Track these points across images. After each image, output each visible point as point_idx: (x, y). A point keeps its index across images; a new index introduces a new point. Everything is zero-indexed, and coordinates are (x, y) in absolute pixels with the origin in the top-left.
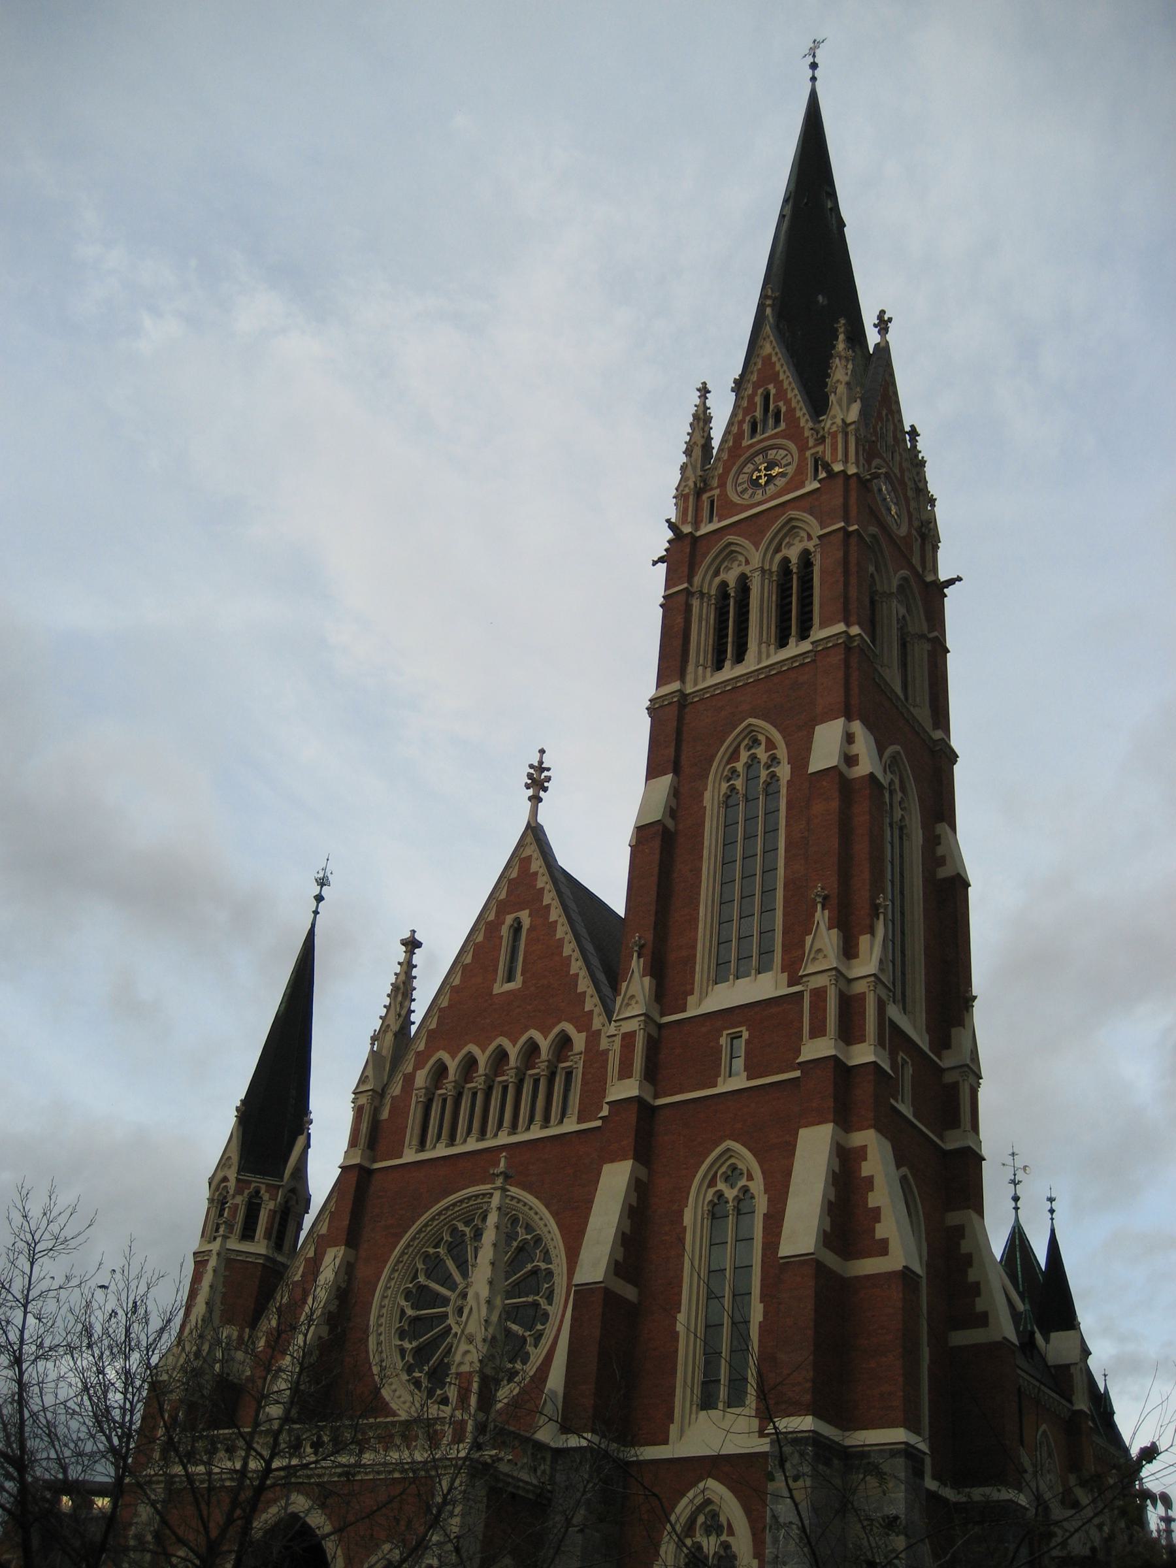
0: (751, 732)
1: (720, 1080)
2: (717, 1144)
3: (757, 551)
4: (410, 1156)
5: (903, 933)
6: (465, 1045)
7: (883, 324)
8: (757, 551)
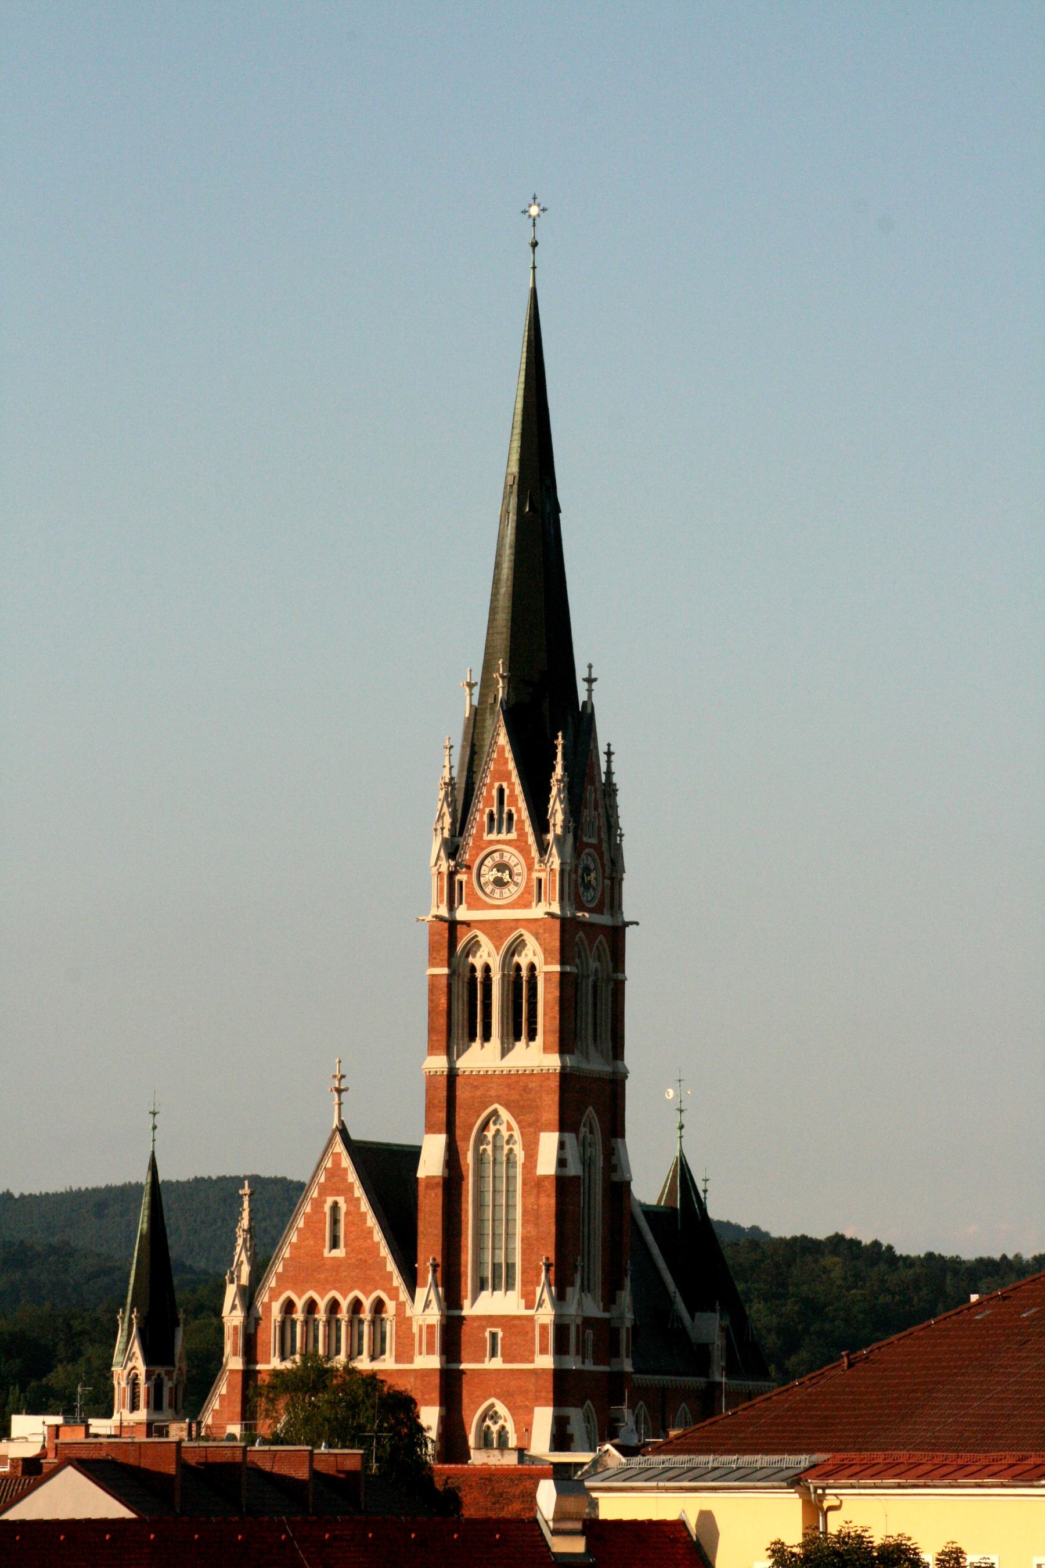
0: (495, 1113)
1: (487, 1359)
2: (486, 1399)
3: (498, 954)
4: (275, 1363)
5: (589, 1279)
6: (308, 1290)
7: (590, 681)
8: (498, 954)
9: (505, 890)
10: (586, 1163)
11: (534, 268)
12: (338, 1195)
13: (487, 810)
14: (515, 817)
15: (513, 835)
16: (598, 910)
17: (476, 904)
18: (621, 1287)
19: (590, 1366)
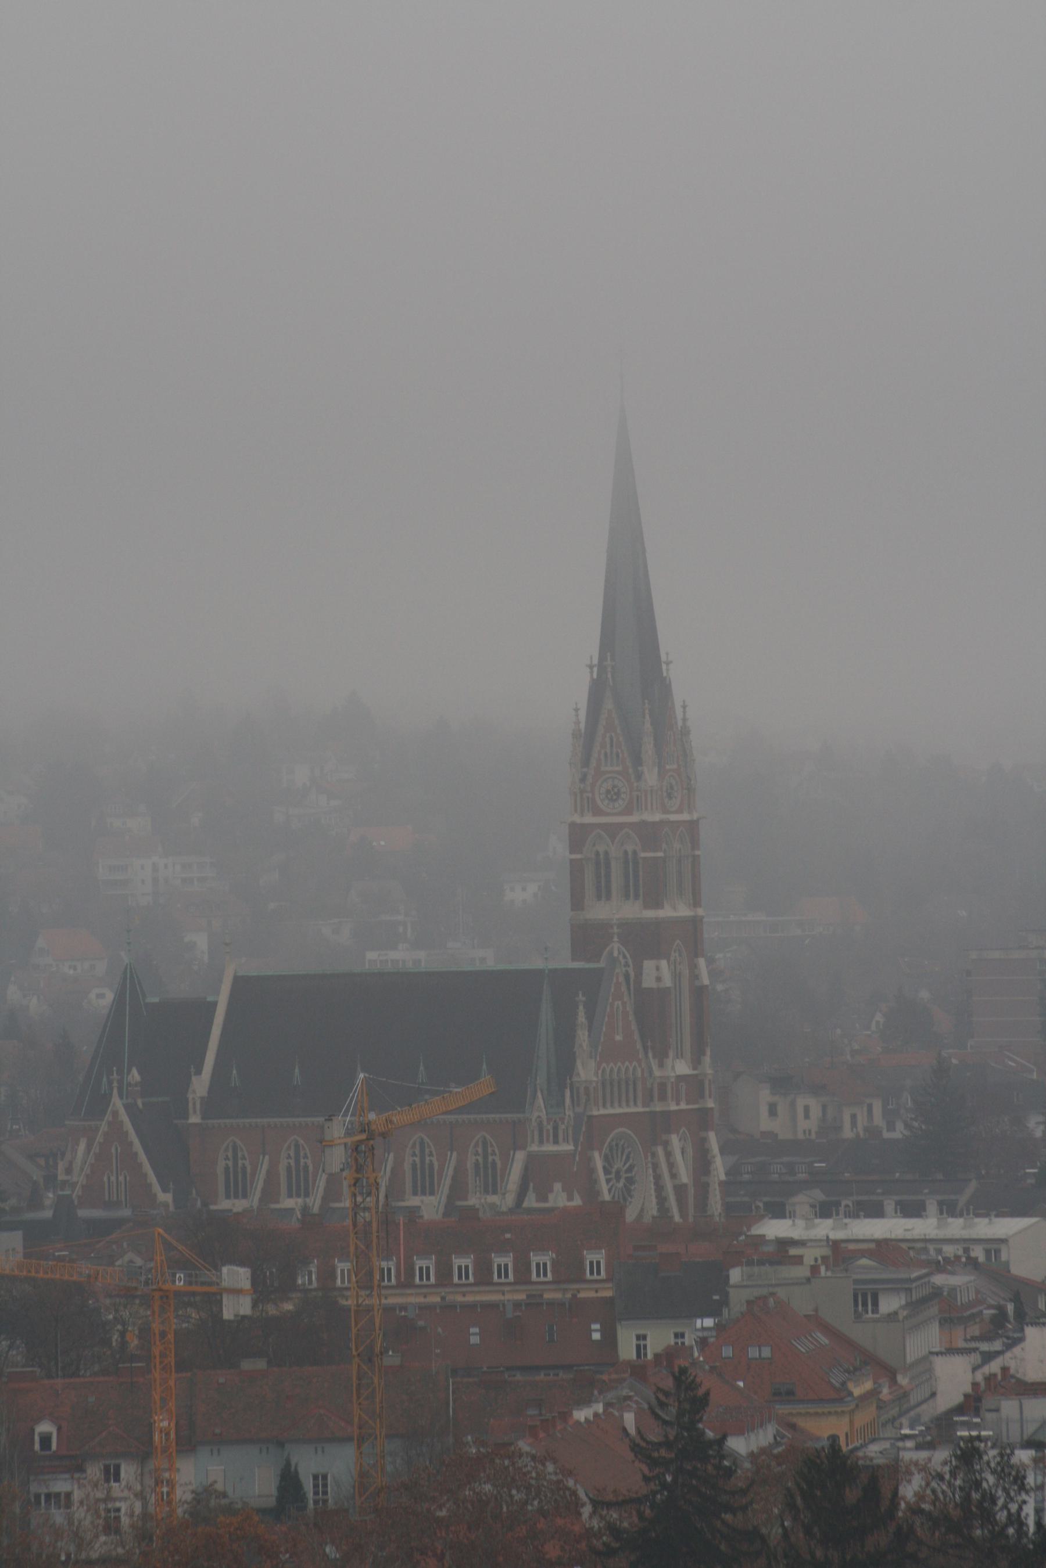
3: (613, 844)
10: (676, 976)
13: (603, 752)
14: (621, 755)
15: (619, 768)
16: (680, 811)
17: (597, 812)
18: (704, 1054)
19: (683, 1106)
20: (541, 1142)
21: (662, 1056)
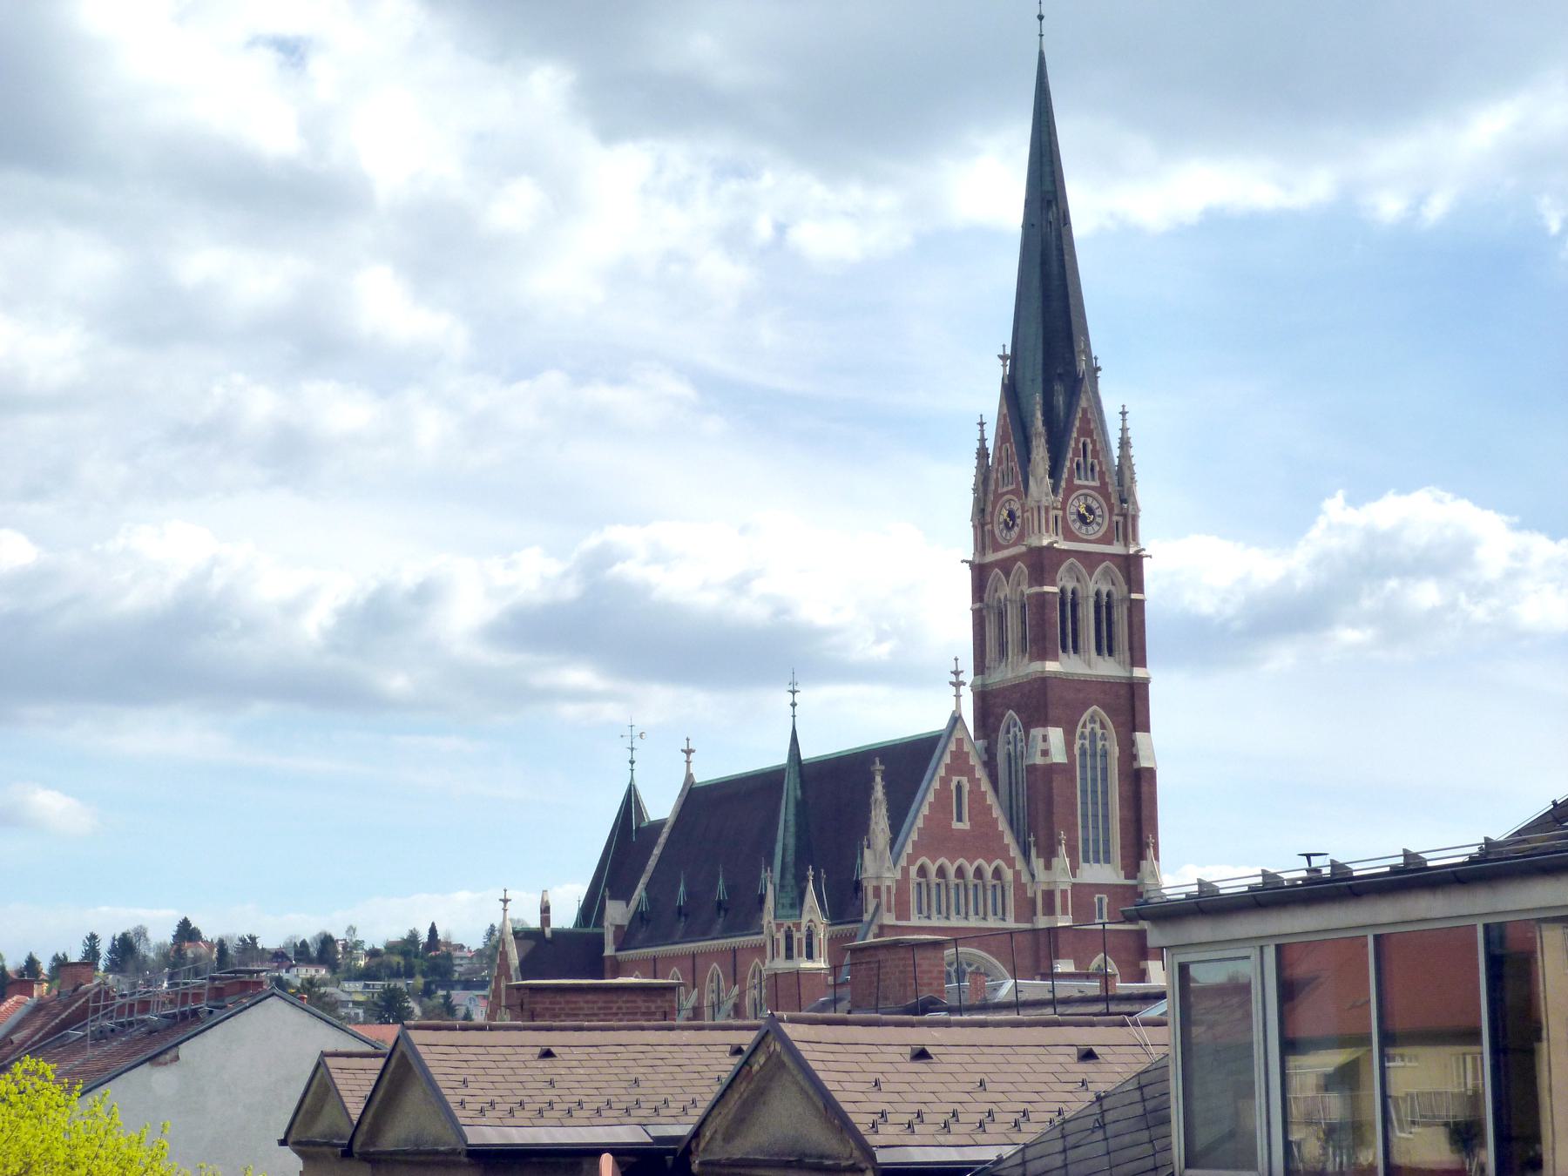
8: (1091, 580)
9: (1090, 528)
11: (1041, 35)
12: (962, 775)
14: (1097, 468)
15: (1096, 483)
17: (1069, 535)
20: (789, 956)
21: (1049, 854)
